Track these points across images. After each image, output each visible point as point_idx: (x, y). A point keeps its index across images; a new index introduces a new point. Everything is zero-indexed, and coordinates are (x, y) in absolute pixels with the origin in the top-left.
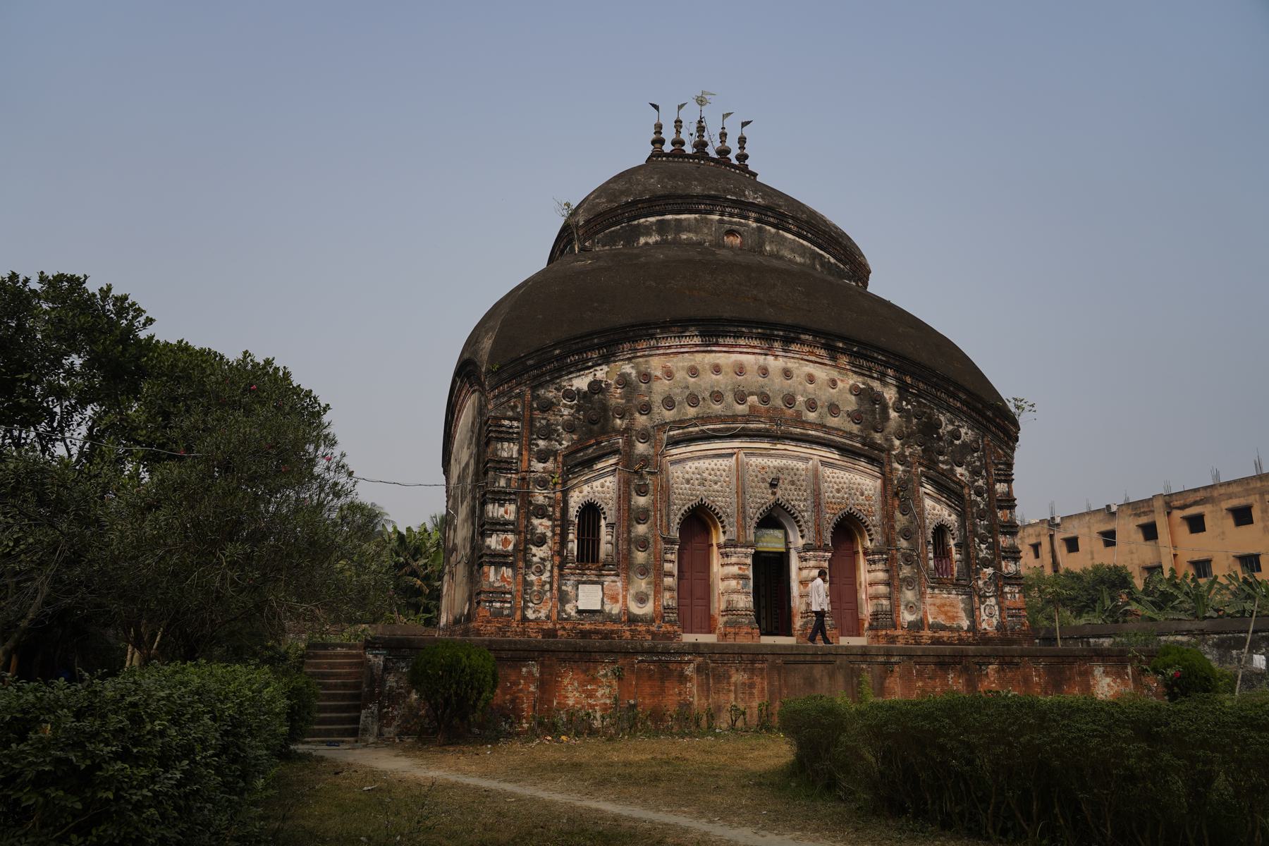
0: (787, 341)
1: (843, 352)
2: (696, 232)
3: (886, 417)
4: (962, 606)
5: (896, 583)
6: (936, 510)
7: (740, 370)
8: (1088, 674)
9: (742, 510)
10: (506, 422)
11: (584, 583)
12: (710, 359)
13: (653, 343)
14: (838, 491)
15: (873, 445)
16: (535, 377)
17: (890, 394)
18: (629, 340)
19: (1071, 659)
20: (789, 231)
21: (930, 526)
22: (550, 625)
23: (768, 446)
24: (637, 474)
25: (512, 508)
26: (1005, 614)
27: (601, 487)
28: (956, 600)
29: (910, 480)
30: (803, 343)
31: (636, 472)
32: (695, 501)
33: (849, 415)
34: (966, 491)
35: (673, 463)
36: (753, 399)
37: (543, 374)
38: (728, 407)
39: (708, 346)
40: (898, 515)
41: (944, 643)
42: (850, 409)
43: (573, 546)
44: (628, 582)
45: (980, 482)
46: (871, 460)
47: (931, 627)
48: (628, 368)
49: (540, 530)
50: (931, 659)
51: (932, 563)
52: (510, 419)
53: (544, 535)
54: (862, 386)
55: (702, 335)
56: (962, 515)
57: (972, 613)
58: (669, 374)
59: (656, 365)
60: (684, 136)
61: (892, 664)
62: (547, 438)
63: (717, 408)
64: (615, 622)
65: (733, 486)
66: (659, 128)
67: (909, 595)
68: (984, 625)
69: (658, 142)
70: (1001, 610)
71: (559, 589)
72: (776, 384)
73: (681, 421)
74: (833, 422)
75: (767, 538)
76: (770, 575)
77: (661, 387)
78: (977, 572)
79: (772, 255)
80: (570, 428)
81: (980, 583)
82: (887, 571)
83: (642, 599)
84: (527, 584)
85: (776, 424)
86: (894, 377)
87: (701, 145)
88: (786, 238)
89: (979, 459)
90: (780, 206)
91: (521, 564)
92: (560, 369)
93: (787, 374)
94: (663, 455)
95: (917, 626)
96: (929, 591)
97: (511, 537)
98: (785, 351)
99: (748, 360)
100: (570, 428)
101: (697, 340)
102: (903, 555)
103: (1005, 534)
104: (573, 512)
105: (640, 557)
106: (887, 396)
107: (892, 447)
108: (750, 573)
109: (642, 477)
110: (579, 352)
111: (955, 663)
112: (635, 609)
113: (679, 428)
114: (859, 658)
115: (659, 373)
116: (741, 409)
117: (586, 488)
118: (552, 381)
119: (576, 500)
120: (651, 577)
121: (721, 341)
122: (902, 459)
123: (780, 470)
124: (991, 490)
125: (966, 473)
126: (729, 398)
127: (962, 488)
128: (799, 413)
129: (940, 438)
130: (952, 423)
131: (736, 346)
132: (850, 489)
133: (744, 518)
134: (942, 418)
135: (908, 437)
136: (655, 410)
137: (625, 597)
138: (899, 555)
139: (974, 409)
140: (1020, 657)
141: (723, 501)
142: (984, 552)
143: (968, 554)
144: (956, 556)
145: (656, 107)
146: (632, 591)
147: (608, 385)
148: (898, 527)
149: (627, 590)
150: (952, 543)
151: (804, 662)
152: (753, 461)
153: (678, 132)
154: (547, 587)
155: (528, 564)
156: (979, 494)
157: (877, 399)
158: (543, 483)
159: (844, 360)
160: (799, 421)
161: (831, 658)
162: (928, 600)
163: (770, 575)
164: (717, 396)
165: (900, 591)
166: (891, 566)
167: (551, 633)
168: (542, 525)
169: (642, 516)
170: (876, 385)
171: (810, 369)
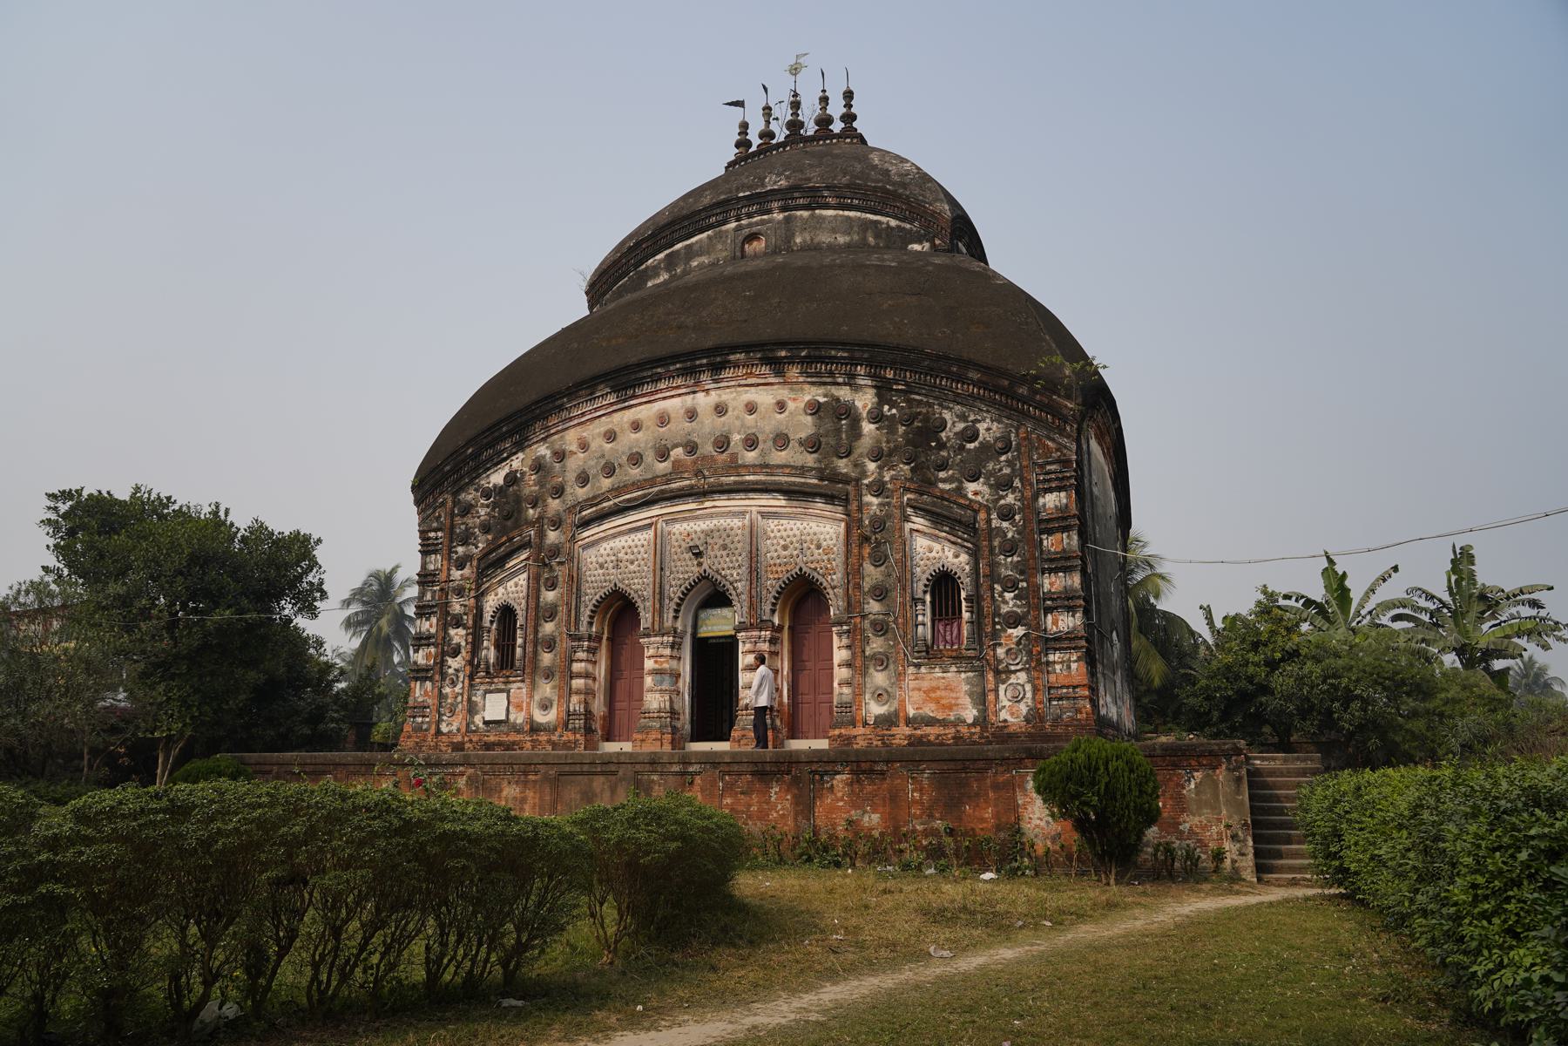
0: (716, 369)
1: (791, 361)
2: (708, 253)
3: (855, 431)
4: (966, 688)
5: (858, 663)
6: (932, 550)
7: (663, 419)
8: (1012, 786)
9: (660, 594)
10: (432, 535)
11: (491, 692)
12: (628, 416)
13: (564, 414)
14: (785, 548)
15: (835, 478)
16: (455, 482)
17: (864, 400)
18: (537, 418)
19: (981, 764)
20: (827, 207)
21: (921, 575)
22: (459, 738)
23: (693, 506)
24: (546, 563)
25: (434, 620)
26: (1039, 697)
27: (511, 589)
28: (958, 681)
29: (889, 516)
30: (736, 365)
31: (545, 565)
32: (609, 587)
33: (801, 443)
34: (982, 516)
35: (585, 547)
36: (678, 453)
37: (462, 477)
38: (649, 468)
39: (625, 401)
40: (868, 567)
41: (930, 743)
42: (803, 435)
43: (490, 653)
44: (533, 687)
45: (1010, 499)
46: (830, 499)
47: (908, 722)
48: (543, 450)
49: (456, 640)
50: (744, 768)
51: (925, 632)
52: (436, 530)
53: (459, 645)
54: (822, 400)
55: (615, 390)
56: (975, 555)
57: (981, 699)
58: (584, 446)
59: (570, 439)
60: (774, 126)
61: (691, 774)
62: (465, 543)
63: (635, 473)
65: (651, 564)
66: (744, 127)
67: (879, 678)
68: (1004, 715)
69: (743, 143)
70: (1035, 690)
71: (469, 699)
72: (709, 424)
73: (594, 497)
74: (779, 457)
75: (713, 620)
76: (714, 665)
77: (574, 464)
78: (995, 635)
79: (805, 248)
80: (486, 528)
81: (1000, 652)
82: (849, 647)
83: (545, 706)
84: (441, 696)
85: (705, 476)
86: (869, 375)
87: (795, 125)
88: (824, 218)
89: (1009, 463)
90: (809, 180)
91: (437, 677)
92: (476, 468)
93: (720, 410)
94: (573, 539)
95: (888, 721)
96: (911, 670)
97: (433, 650)
98: (716, 381)
99: (675, 405)
100: (486, 528)
101: (612, 398)
102: (874, 624)
103: (1055, 571)
104: (487, 617)
105: (546, 658)
106: (859, 404)
107: (864, 474)
108: (686, 668)
109: (551, 569)
110: (491, 445)
111: (783, 773)
112: (540, 717)
113: (592, 506)
114: (648, 767)
115: (574, 448)
116: (663, 467)
117: (501, 590)
118: (471, 482)
119: (491, 603)
120: (556, 682)
121: (638, 392)
122: (879, 489)
123: (708, 533)
124: (1030, 506)
125: (986, 489)
126: (649, 457)
127: (976, 512)
128: (734, 457)
129: (942, 446)
130: (963, 418)
131: (657, 392)
132: (802, 542)
133: (661, 600)
134: (947, 415)
135: (890, 455)
136: (568, 490)
137: (529, 704)
138: (867, 624)
139: (997, 389)
140: (887, 762)
141: (639, 585)
142: (1009, 603)
143: (980, 609)
144: (966, 615)
145: (739, 104)
146: (537, 698)
147: (523, 474)
148: (866, 586)
149: (531, 697)
150: (963, 594)
151: (582, 773)
152: (679, 528)
153: (768, 122)
155: (443, 675)
156: (1007, 514)
157: (846, 412)
158: (460, 592)
159: (794, 372)
160: (734, 466)
161: (613, 768)
162: (910, 682)
163: (714, 665)
164: (636, 459)
165: (864, 674)
166: (853, 640)
167: (458, 747)
168: (458, 635)
169: (551, 613)
170: (844, 393)
171: (752, 395)
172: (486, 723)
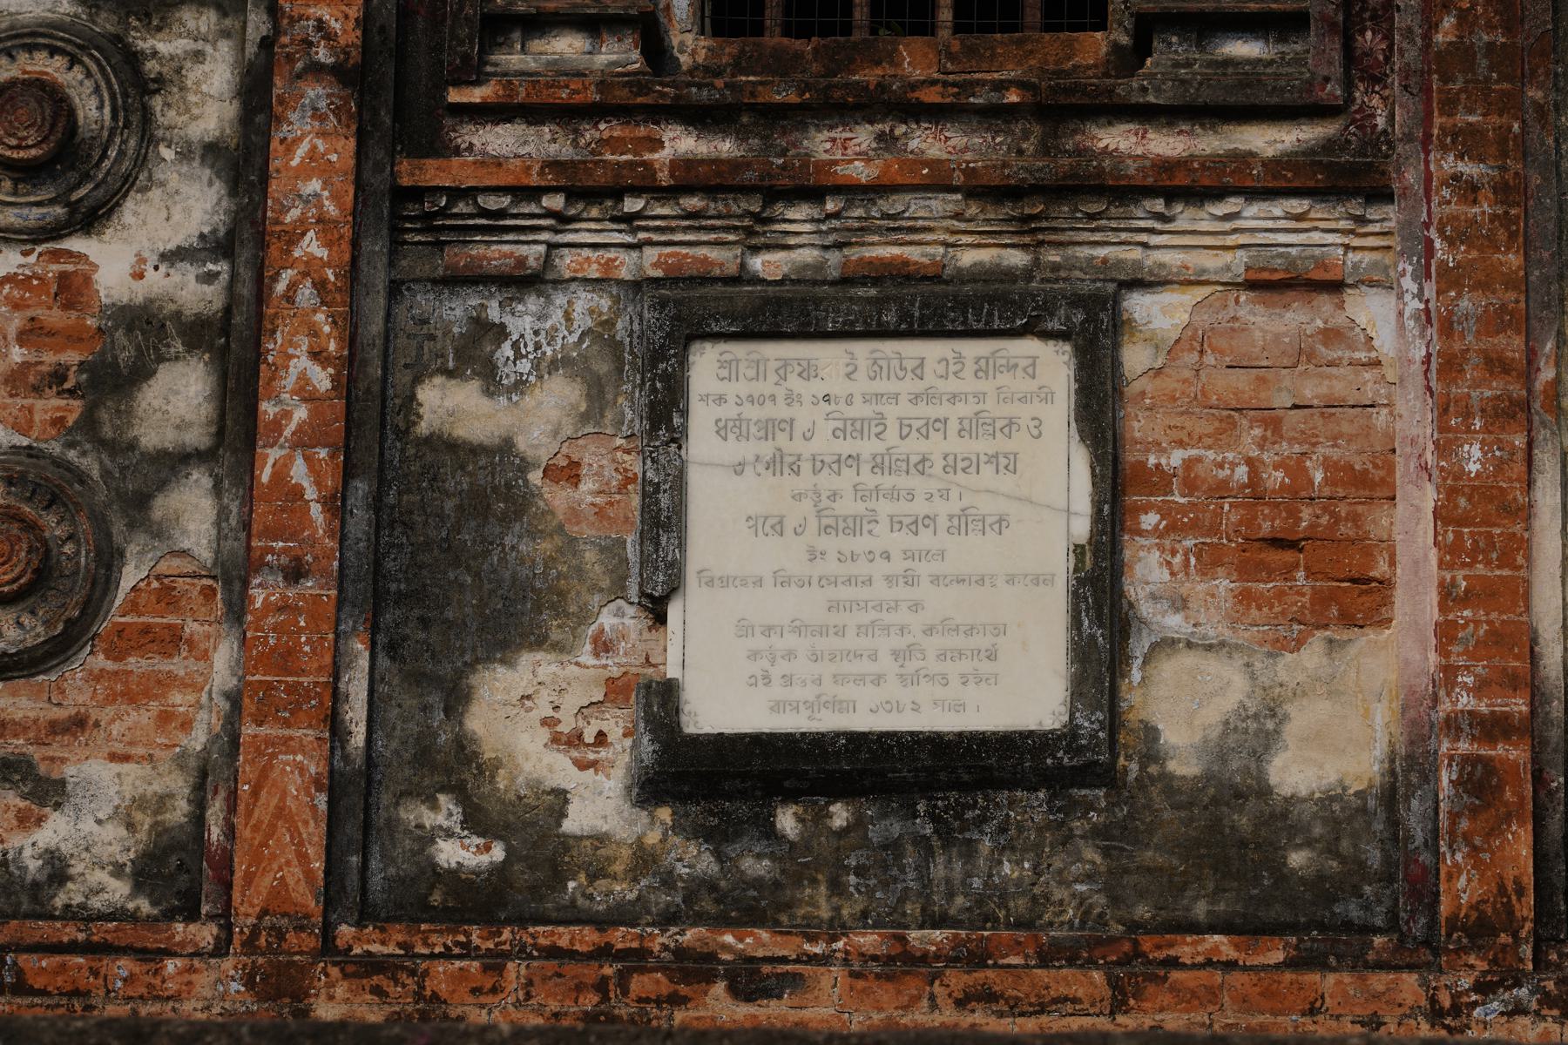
64: (1321, 927)
71: (370, 417)
154: (178, 398)
172: (706, 778)
